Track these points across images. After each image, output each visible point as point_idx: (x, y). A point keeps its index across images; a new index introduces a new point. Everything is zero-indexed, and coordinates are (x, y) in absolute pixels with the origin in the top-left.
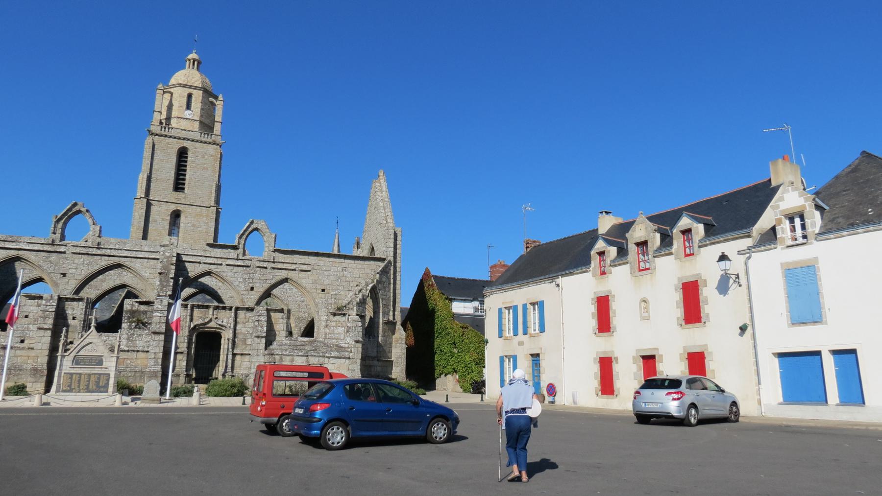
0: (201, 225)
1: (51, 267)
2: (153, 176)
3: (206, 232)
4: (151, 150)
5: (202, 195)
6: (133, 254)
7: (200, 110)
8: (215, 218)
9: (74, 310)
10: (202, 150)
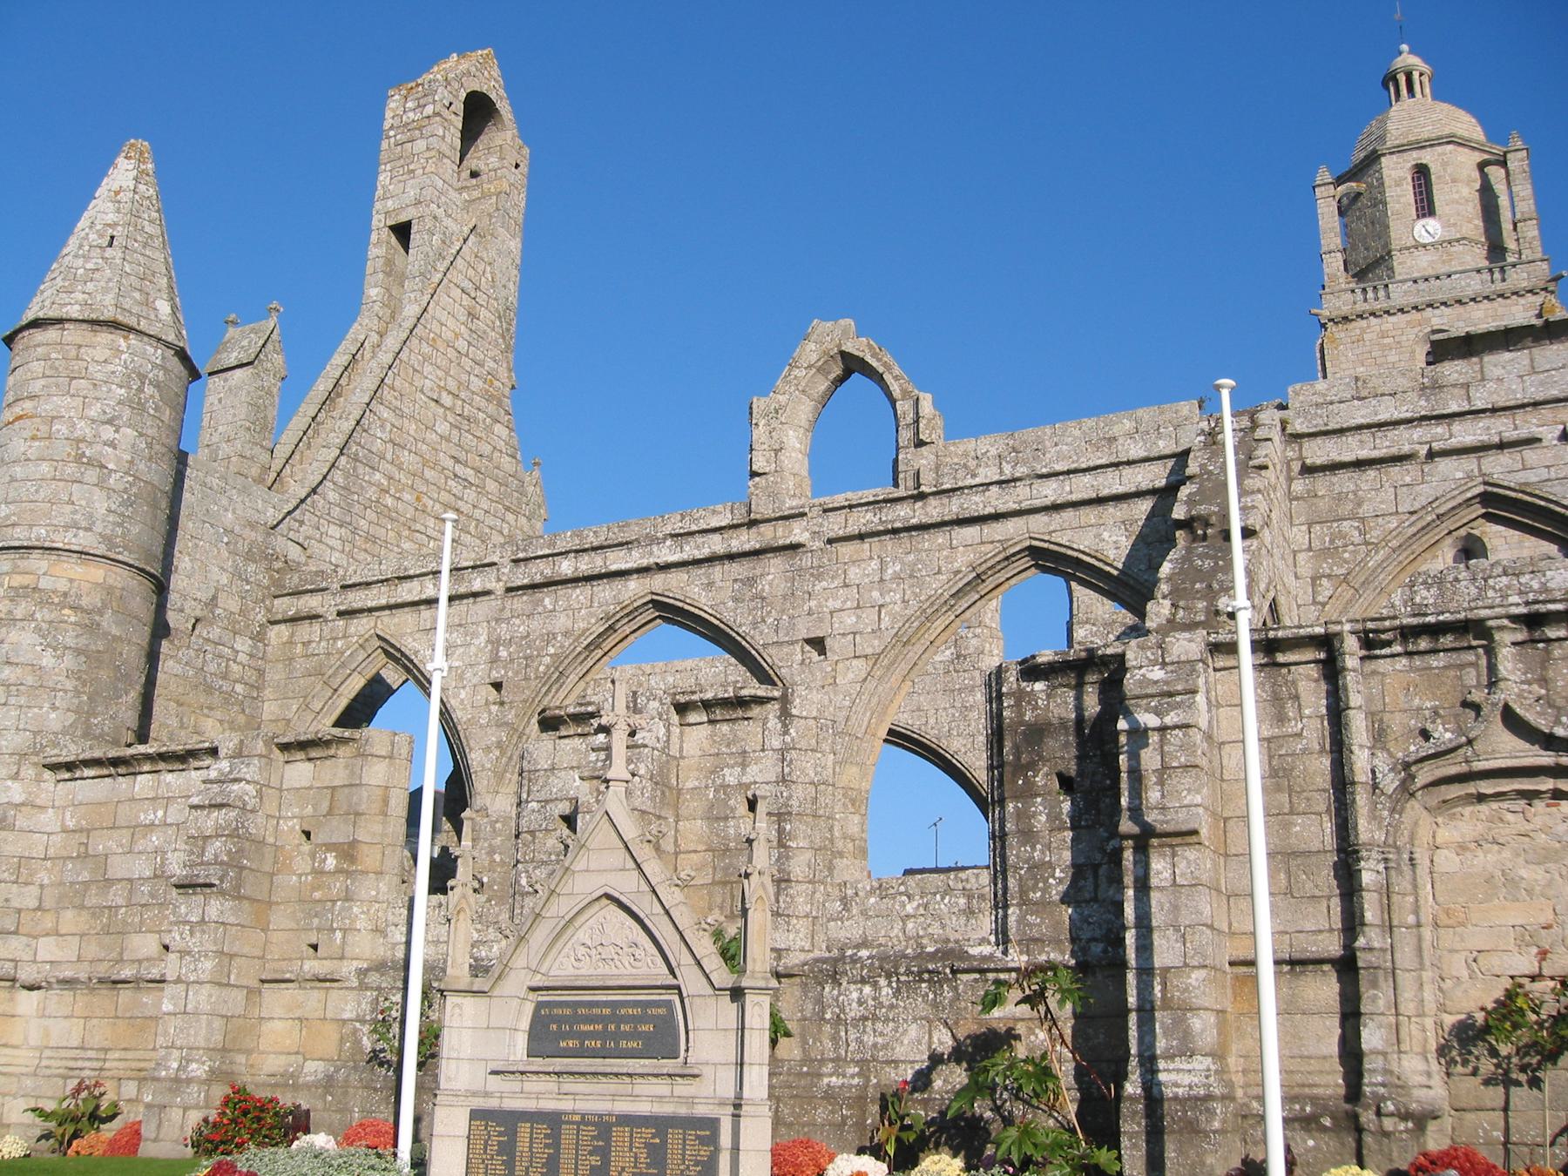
6: (1083, 487)
9: (744, 766)
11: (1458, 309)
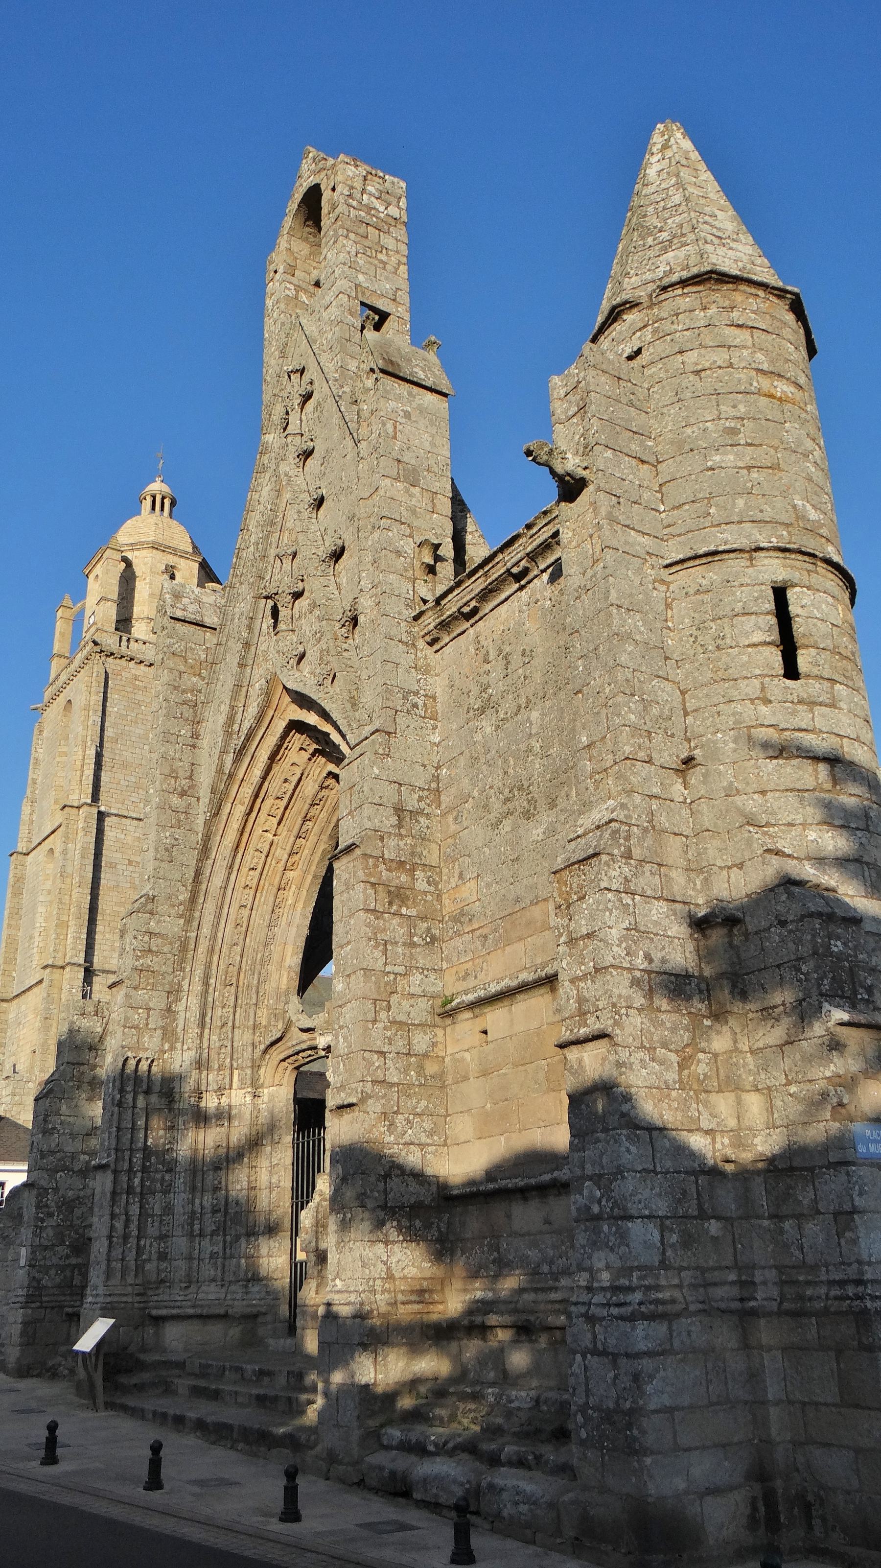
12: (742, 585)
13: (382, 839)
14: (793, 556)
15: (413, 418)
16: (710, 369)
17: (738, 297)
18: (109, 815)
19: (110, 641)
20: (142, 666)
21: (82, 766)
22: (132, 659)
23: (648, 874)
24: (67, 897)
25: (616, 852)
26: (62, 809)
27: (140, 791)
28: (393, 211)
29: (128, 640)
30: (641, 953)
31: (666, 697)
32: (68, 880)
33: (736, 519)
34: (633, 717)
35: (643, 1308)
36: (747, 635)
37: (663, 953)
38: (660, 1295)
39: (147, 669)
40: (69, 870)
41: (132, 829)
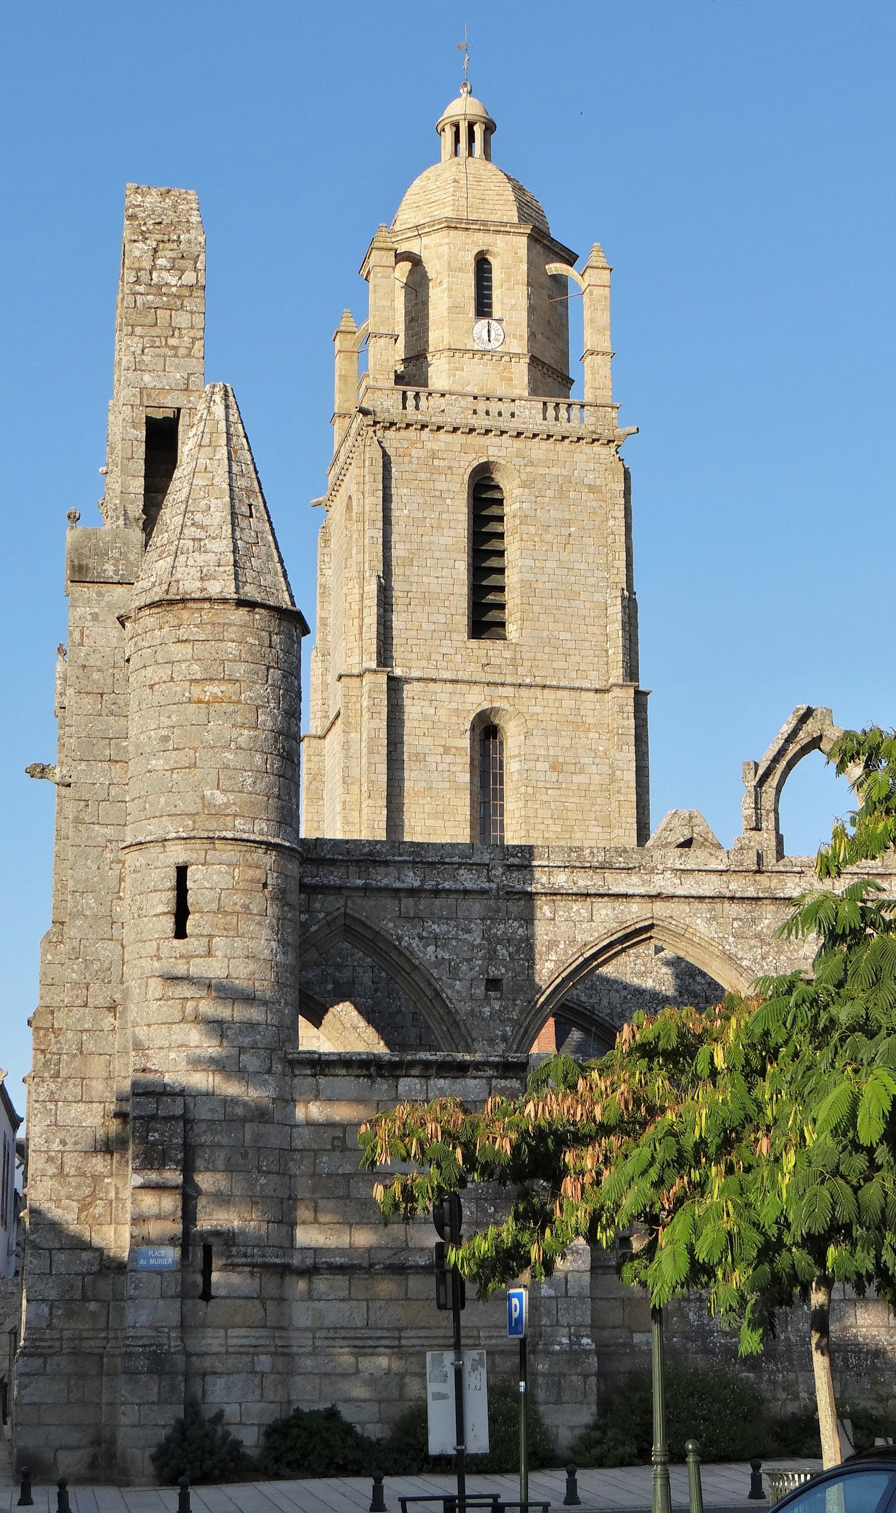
0: (583, 761)
1: (763, 958)
2: (398, 586)
3: (605, 789)
4: (381, 486)
5: (572, 645)
7: (525, 314)
8: (633, 731)
10: (555, 471)
11: (519, 443)
12: (156, 868)
13: (52, 1013)
14: (193, 841)
15: (101, 618)
16: (159, 683)
17: (185, 614)
18: (407, 680)
19: (388, 404)
20: (442, 435)
21: (361, 610)
22: (424, 427)
23: (71, 1086)
24: (356, 814)
25: (46, 1075)
26: (340, 677)
27: (455, 636)
28: (189, 278)
29: (417, 396)
30: (58, 1140)
31: (107, 953)
32: (355, 789)
33: (158, 814)
34: (74, 975)
35: (26, 1350)
36: (154, 907)
37: (77, 1138)
38: (43, 1344)
39: (450, 436)
40: (355, 772)
41: (444, 697)
